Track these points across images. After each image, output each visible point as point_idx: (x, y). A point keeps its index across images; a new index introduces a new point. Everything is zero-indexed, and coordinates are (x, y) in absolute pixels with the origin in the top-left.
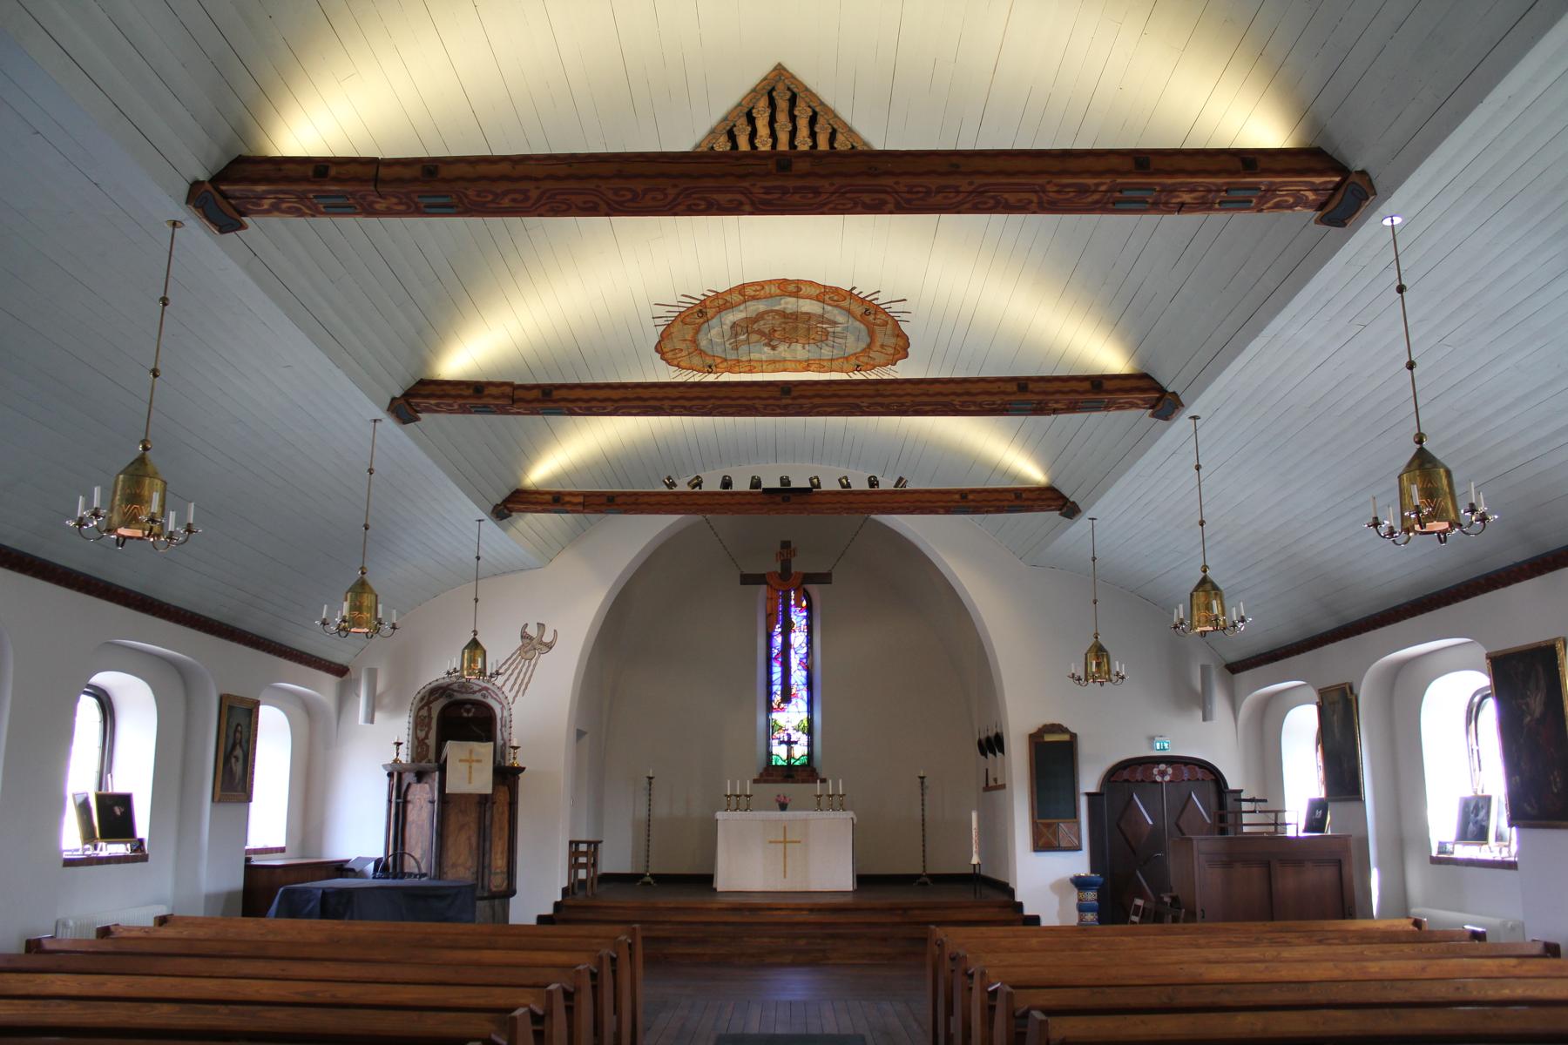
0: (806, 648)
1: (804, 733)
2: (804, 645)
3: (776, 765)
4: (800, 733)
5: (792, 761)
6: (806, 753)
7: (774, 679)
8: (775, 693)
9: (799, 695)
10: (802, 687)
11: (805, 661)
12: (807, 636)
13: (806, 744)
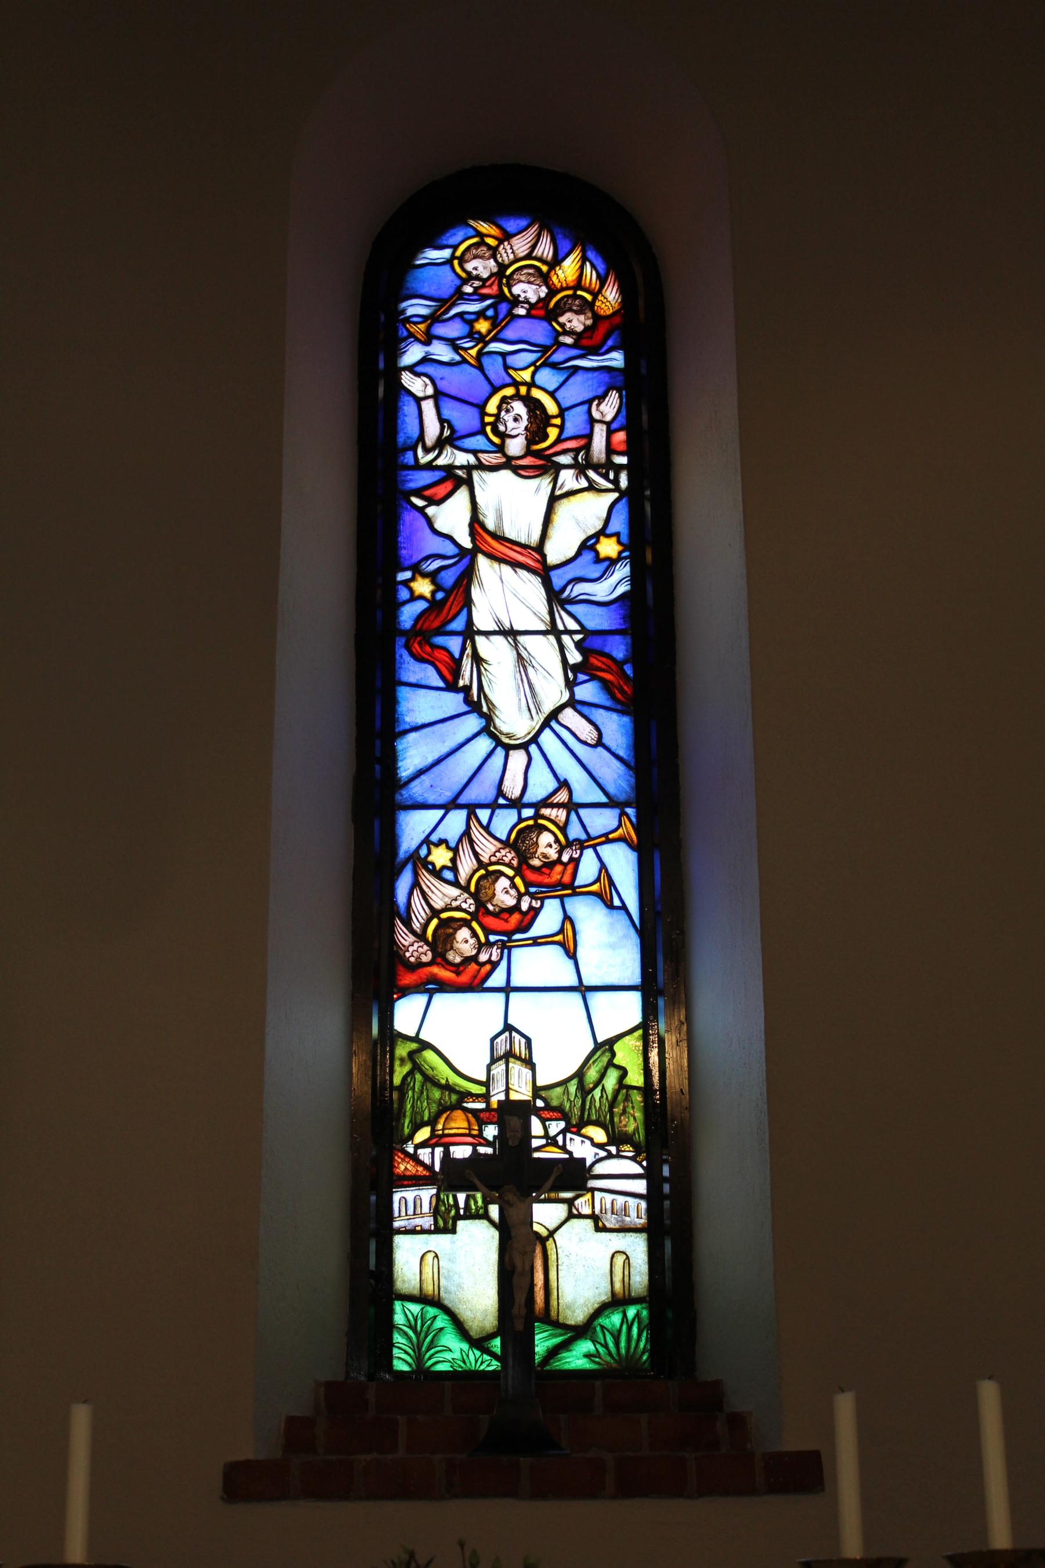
0: (622, 571)
1: (617, 1138)
2: (608, 548)
3: (422, 1374)
4: (599, 1135)
5: (543, 1342)
6: (640, 1277)
7: (407, 766)
8: (419, 862)
9: (588, 870)
10: (601, 821)
11: (618, 649)
12: (631, 497)
13: (637, 1211)
